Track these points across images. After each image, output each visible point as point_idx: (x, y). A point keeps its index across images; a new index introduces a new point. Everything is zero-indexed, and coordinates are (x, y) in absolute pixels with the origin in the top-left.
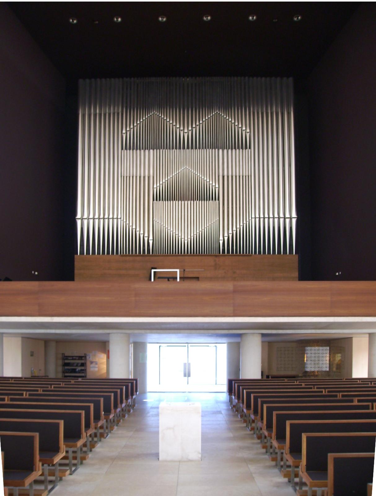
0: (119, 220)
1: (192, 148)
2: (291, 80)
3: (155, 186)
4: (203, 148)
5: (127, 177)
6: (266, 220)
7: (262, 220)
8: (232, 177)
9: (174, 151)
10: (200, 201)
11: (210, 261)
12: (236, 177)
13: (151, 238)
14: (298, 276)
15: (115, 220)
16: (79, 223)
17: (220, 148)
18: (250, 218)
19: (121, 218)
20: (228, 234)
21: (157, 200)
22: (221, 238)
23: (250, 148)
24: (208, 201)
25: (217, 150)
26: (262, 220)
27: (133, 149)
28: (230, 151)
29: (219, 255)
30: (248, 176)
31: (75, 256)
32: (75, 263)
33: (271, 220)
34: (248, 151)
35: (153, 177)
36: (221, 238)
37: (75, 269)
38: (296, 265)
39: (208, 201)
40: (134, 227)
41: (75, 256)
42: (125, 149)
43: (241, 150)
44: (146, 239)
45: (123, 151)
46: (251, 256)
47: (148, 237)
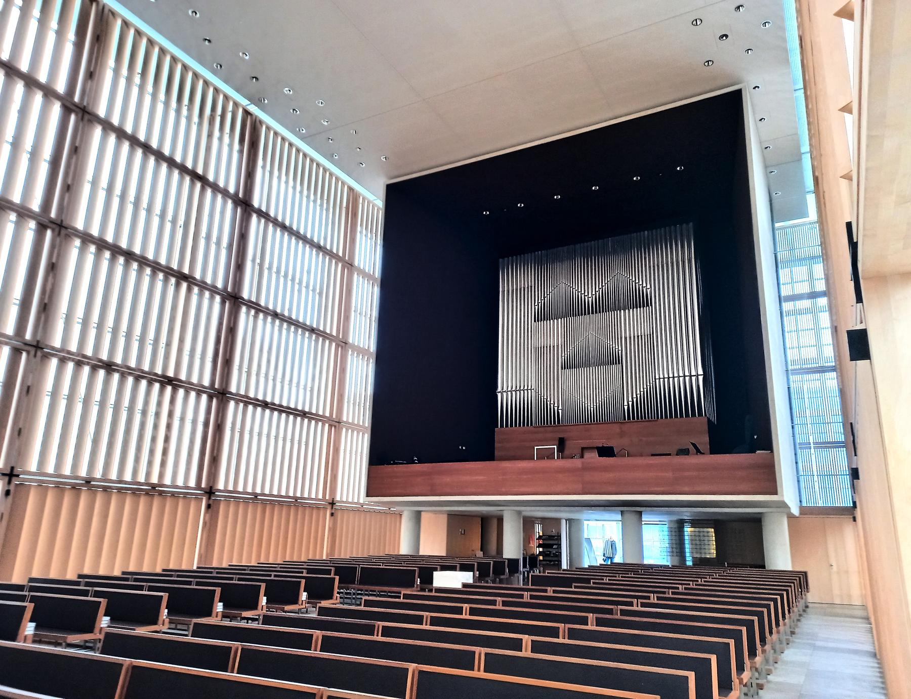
3: (563, 355)
16: (499, 395)
22: (626, 403)
36: (626, 403)
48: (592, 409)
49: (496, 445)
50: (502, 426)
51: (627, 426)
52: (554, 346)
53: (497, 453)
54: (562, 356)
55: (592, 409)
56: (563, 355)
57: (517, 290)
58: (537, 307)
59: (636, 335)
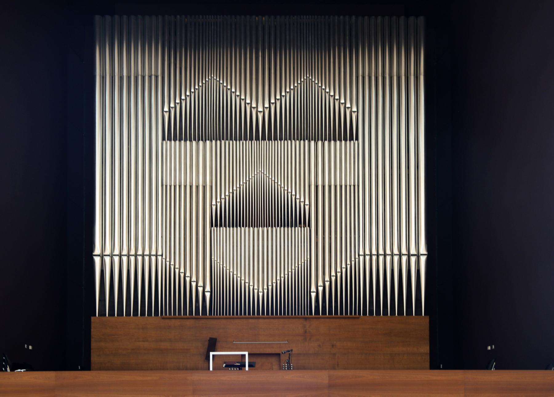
0: (160, 258)
1: (270, 139)
2: (421, 20)
3: (214, 203)
4: (286, 139)
5: (170, 186)
6: (381, 258)
7: (374, 258)
8: (330, 187)
9: (243, 143)
10: (282, 228)
11: (296, 326)
12: (336, 186)
13: (208, 288)
14: (429, 352)
15: (153, 258)
16: (97, 260)
17: (312, 140)
18: (357, 256)
19: (162, 255)
20: (324, 282)
21: (216, 226)
22: (313, 289)
23: (357, 139)
24: (293, 228)
25: (307, 142)
26: (374, 258)
27: (180, 140)
28: (326, 143)
29: (311, 316)
30: (354, 186)
31: (93, 318)
32: (92, 330)
33: (388, 258)
34: (354, 144)
35: (211, 187)
36: (313, 289)
37: (92, 340)
38: (426, 333)
39: (293, 228)
40: (182, 270)
41: (93, 318)
42: (168, 140)
43: (343, 142)
44: (200, 289)
45: (164, 142)
46: (358, 318)
47: (204, 287)
48: (261, 294)
49: (94, 345)
50: (102, 313)
51: (315, 323)
52: (197, 187)
53: (95, 358)
55: (261, 294)
56: (214, 203)
57: (129, 78)
58: (166, 116)
59: (348, 184)
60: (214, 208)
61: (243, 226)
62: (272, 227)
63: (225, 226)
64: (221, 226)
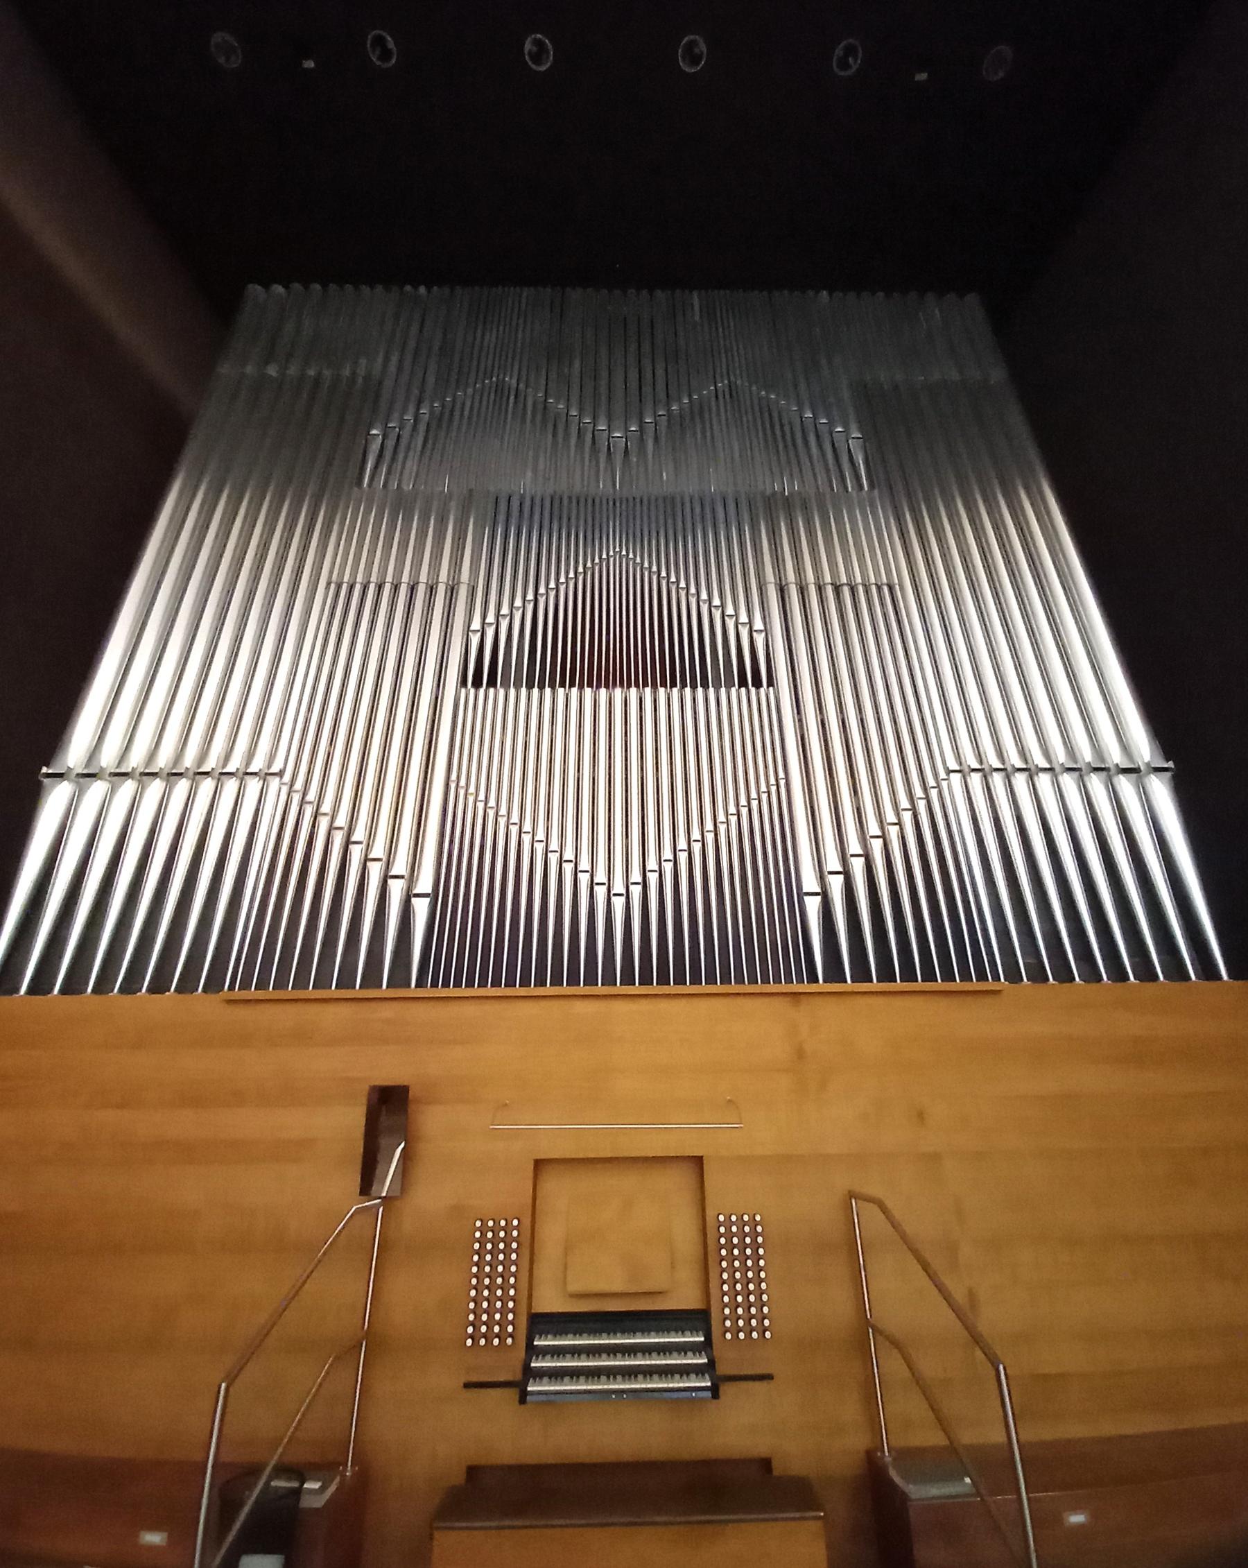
3: (476, 625)
10: (688, 690)
13: (425, 884)
19: (280, 774)
22: (810, 882)
24: (723, 690)
47: (412, 878)
48: (618, 903)
54: (468, 630)
55: (618, 903)
56: (476, 625)
60: (475, 640)
61: (563, 685)
62: (654, 687)
63: (506, 685)
64: (492, 682)
